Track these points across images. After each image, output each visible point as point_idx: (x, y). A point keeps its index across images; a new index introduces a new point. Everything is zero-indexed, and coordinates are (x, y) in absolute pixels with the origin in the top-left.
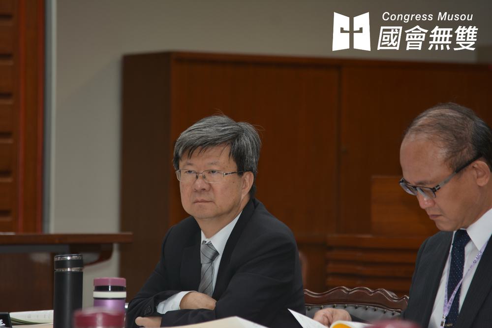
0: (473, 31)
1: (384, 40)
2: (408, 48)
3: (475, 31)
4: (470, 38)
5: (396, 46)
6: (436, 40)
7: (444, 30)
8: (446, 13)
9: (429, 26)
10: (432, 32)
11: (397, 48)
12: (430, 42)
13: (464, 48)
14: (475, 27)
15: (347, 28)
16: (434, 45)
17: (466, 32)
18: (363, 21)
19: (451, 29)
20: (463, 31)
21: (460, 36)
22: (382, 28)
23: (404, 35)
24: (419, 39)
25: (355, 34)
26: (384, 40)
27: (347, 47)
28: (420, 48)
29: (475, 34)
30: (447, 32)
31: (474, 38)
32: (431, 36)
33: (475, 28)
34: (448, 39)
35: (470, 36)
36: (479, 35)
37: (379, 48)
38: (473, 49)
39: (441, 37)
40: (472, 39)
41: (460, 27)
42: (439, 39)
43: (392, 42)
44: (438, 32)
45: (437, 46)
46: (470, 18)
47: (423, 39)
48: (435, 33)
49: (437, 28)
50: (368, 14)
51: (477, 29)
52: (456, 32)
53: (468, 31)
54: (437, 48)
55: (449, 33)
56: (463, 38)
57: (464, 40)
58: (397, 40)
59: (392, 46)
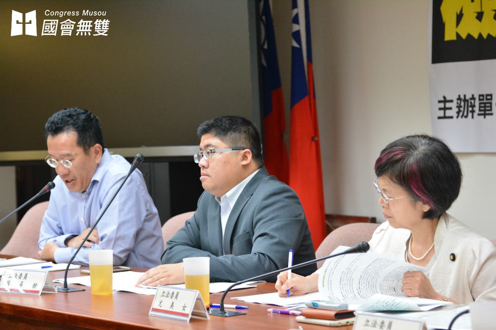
1: (46, 29)
2: (62, 35)
4: (104, 27)
5: (54, 33)
6: (81, 29)
7: (87, 22)
8: (88, 11)
9: (76, 19)
10: (79, 23)
11: (55, 34)
12: (77, 30)
13: (100, 34)
14: (107, 20)
15: (21, 21)
16: (80, 32)
18: (32, 16)
19: (92, 22)
22: (45, 21)
23: (59, 26)
24: (70, 28)
26: (46, 29)
27: (22, 34)
28: (70, 35)
30: (88, 24)
32: (78, 26)
33: (107, 21)
34: (89, 28)
36: (110, 25)
37: (43, 34)
38: (106, 35)
39: (84, 27)
40: (106, 28)
41: (97, 20)
43: (52, 31)
44: (82, 24)
45: (82, 33)
46: (104, 14)
47: (73, 28)
48: (81, 24)
49: (82, 21)
50: (34, 12)
51: (109, 22)
53: (103, 23)
54: (82, 34)
55: (90, 24)
58: (55, 29)
59: (51, 33)
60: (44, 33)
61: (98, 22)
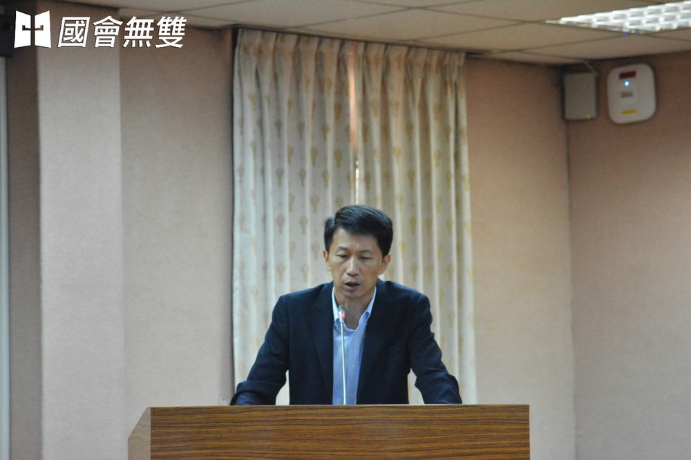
0: (180, 23)
1: (66, 34)
2: (97, 45)
3: (183, 23)
4: (176, 32)
5: (82, 42)
6: (133, 34)
7: (144, 21)
10: (128, 24)
11: (84, 45)
12: (126, 37)
13: (168, 44)
14: (182, 18)
16: (131, 40)
17: (172, 24)
20: (167, 23)
21: (163, 30)
23: (92, 28)
24: (111, 33)
25: (30, 28)
26: (66, 34)
28: (112, 45)
29: (182, 27)
30: (146, 24)
31: (182, 32)
32: (127, 29)
33: (182, 20)
34: (148, 33)
35: (177, 29)
37: (60, 44)
38: (180, 46)
40: (179, 34)
41: (163, 18)
42: (136, 34)
43: (77, 38)
44: (135, 24)
45: (134, 42)
48: (132, 26)
52: (158, 24)
54: (134, 45)
56: (168, 32)
57: (169, 34)
59: (77, 41)
60: (63, 42)
61: (164, 22)
